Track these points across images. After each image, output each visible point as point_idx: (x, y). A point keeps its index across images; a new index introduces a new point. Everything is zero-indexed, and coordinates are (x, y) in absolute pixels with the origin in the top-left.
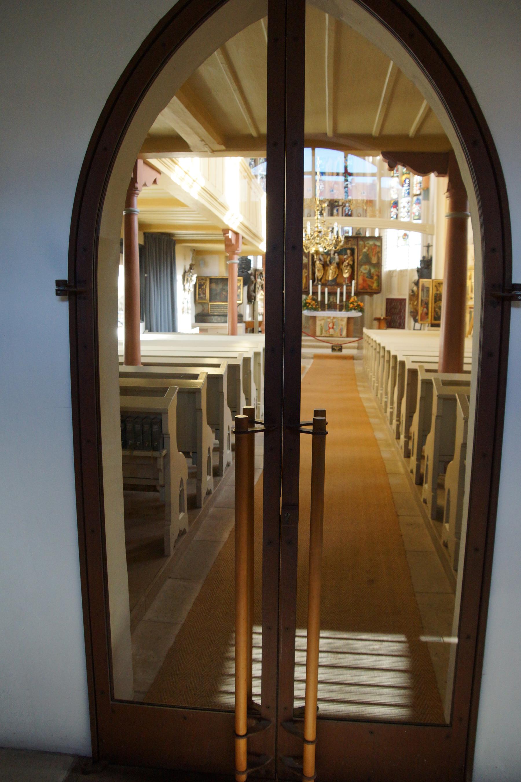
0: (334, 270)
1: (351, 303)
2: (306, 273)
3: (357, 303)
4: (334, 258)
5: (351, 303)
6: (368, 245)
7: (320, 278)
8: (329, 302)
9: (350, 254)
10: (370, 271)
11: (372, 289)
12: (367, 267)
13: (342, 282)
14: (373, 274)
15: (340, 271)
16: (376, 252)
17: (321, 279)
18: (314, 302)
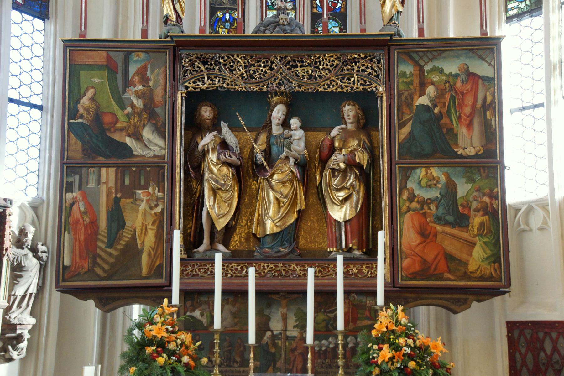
0: (286, 190)
1: (381, 340)
2: (154, 202)
3: (410, 341)
4: (287, 141)
5: (381, 340)
6: (435, 78)
7: (221, 224)
8: (269, 333)
9: (357, 120)
10: (451, 188)
11: (466, 276)
12: (435, 172)
13: (324, 245)
14: (467, 206)
15: (313, 199)
16: (473, 106)
17: (229, 229)
18: (186, 337)
